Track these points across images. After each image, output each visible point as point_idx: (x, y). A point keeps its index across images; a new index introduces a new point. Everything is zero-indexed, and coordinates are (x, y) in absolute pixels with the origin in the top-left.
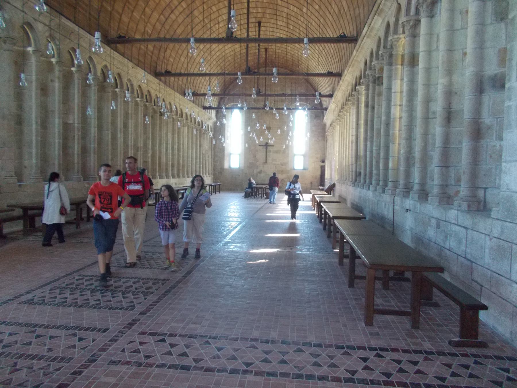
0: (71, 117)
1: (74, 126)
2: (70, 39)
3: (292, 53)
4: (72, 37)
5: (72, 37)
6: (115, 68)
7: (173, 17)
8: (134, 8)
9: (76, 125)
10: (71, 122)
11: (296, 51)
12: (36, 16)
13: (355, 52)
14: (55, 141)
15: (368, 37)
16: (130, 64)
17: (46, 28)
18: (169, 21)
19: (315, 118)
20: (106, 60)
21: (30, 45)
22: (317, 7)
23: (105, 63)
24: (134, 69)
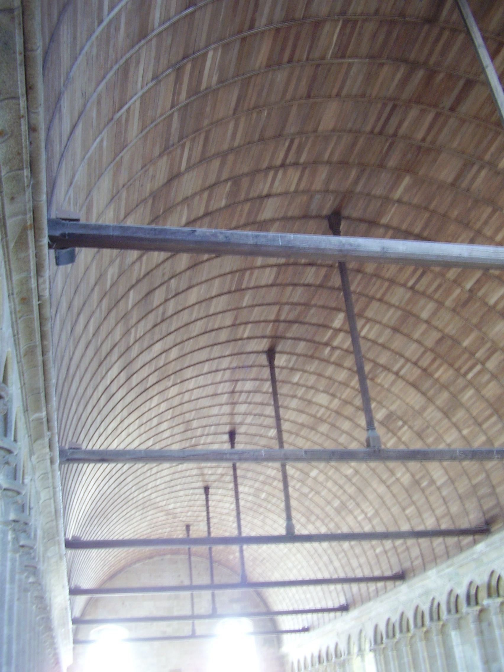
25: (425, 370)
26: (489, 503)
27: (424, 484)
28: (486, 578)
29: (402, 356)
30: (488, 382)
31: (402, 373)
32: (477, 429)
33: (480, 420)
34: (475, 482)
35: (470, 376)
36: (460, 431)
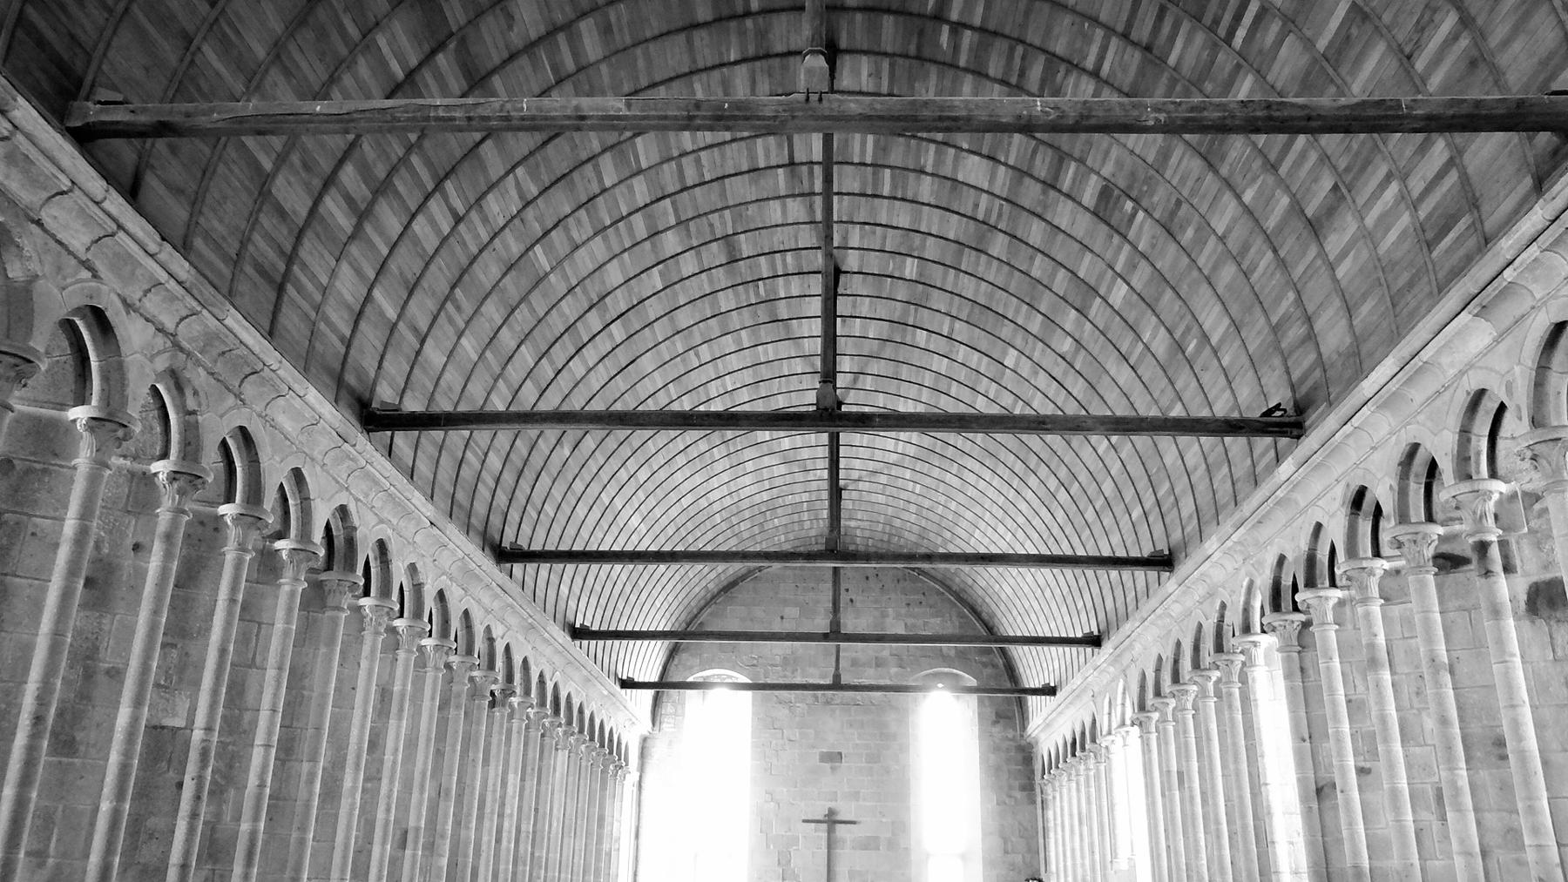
0: (183, 705)
1: (187, 744)
2: (238, 396)
3: (927, 503)
4: (249, 390)
5: (249, 390)
6: (372, 520)
7: (577, 367)
8: (468, 323)
9: (197, 735)
10: (179, 722)
11: (942, 499)
12: (134, 294)
13: (1287, 467)
14: (96, 809)
15: (1383, 406)
16: (428, 510)
17: (160, 341)
18: (564, 382)
19: (995, 723)
20: (347, 489)
21: (82, 399)
22: (1066, 346)
23: (342, 499)
24: (435, 531)
25: (1148, 48)
26: (1303, 362)
27: (1191, 348)
28: (1304, 545)
29: (1095, 21)
30: (1279, 42)
31: (1105, 70)
32: (1270, 179)
33: (1272, 157)
34: (1274, 320)
35: (1241, 34)
36: (1238, 197)
